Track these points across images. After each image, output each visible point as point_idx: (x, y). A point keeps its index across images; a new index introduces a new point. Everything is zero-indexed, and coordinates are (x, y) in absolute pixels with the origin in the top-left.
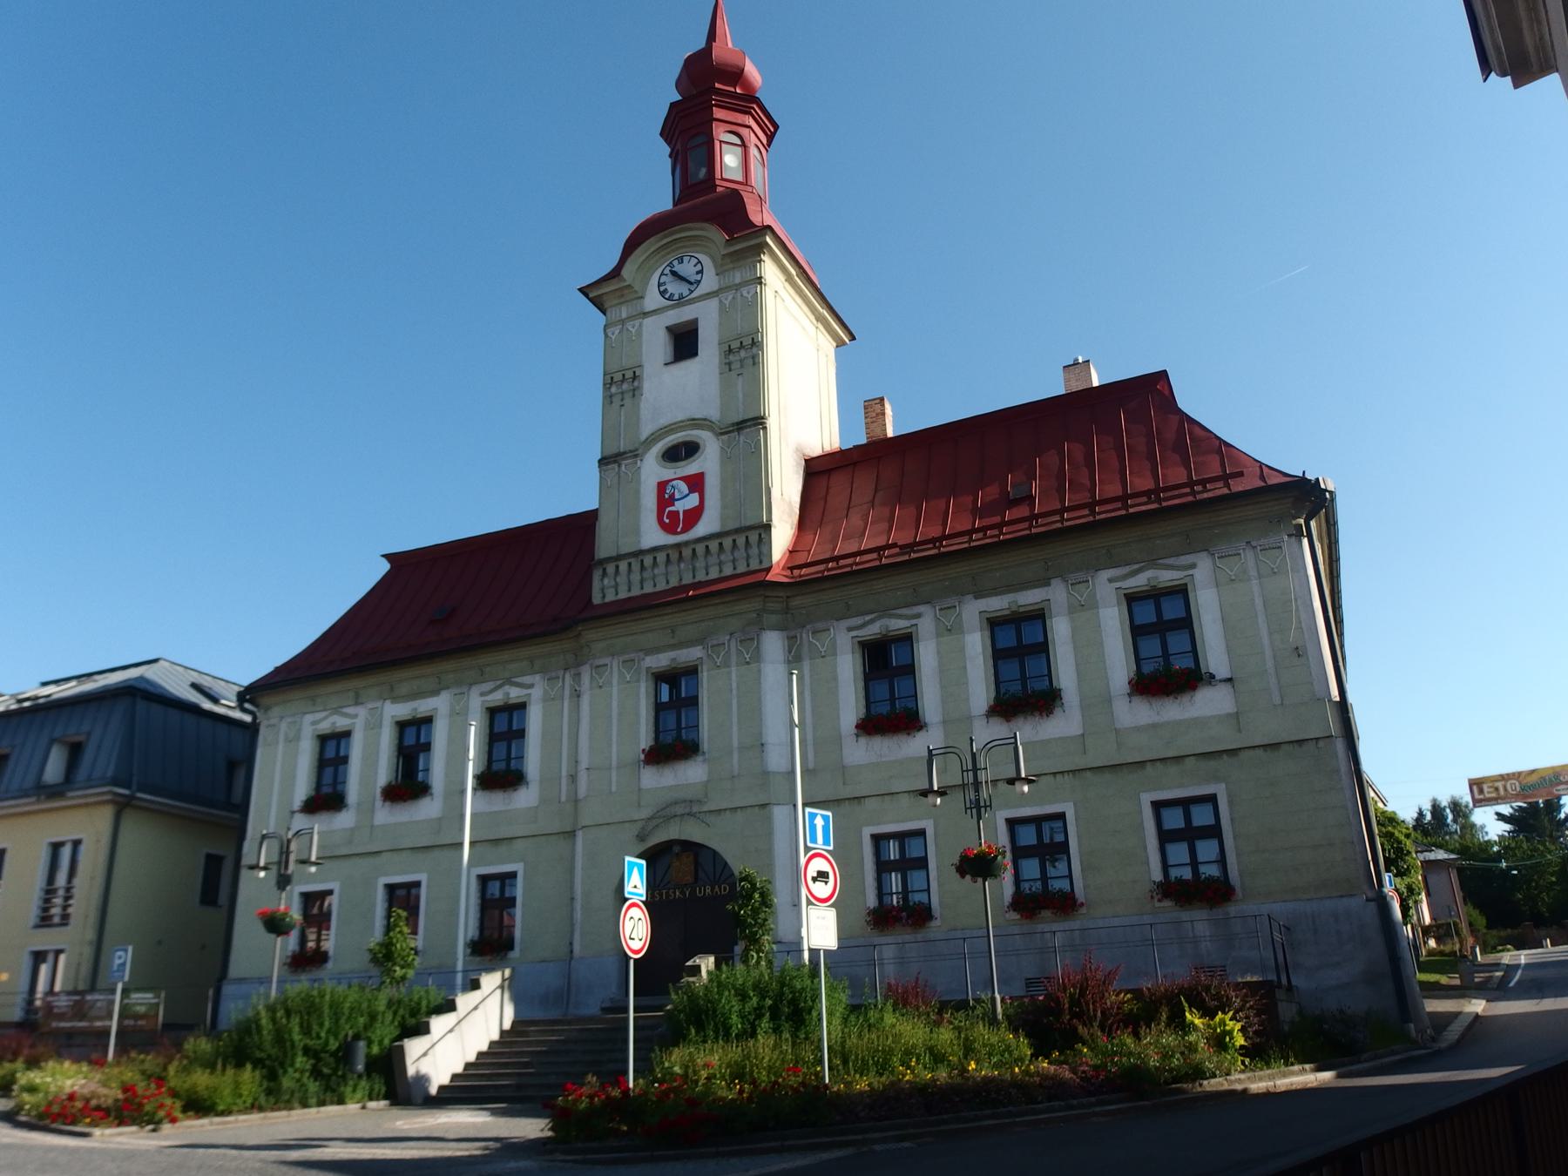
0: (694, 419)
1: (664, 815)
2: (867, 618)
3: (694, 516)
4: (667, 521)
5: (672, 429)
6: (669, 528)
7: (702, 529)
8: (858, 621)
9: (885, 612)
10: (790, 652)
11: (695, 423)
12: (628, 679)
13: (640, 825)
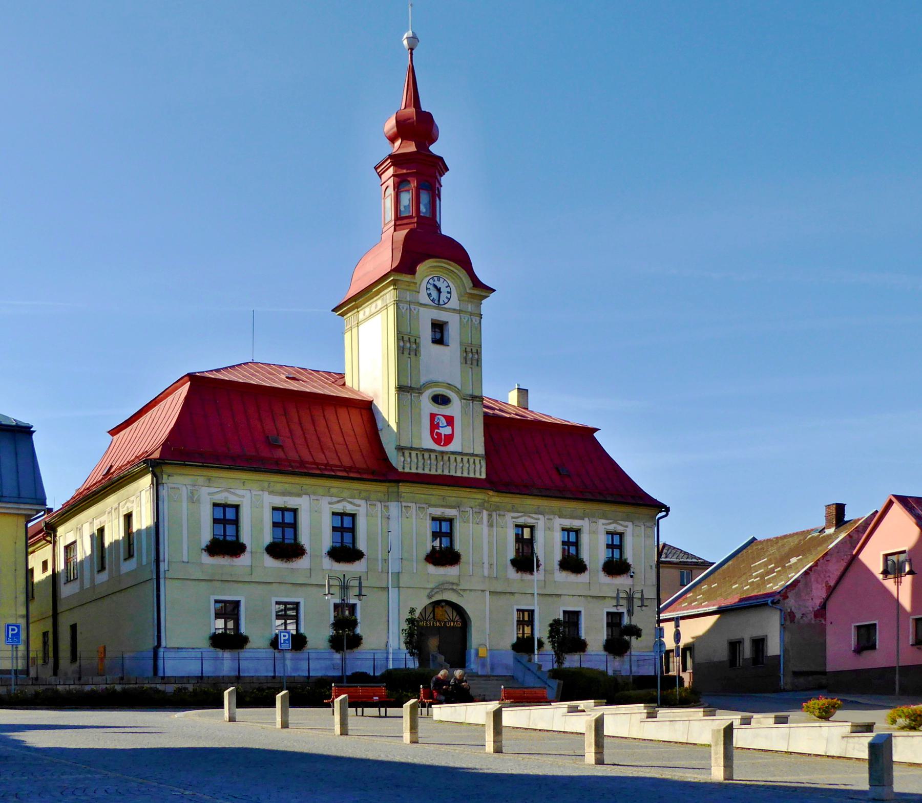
0: (449, 384)
1: (441, 587)
2: (520, 514)
3: (449, 439)
4: (436, 437)
5: (438, 385)
6: (437, 440)
7: (451, 447)
8: (516, 515)
9: (526, 513)
10: (488, 522)
11: (450, 386)
12: (422, 517)
13: (429, 591)
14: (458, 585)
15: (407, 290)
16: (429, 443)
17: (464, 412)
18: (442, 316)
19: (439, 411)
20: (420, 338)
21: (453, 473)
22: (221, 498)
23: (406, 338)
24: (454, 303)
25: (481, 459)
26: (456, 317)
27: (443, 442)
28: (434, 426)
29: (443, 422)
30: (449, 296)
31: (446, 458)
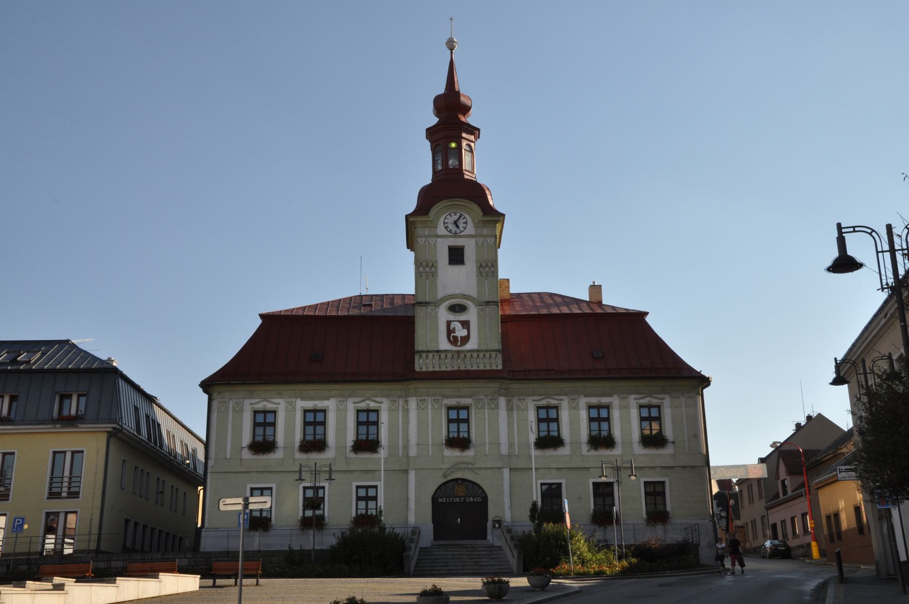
3: (465, 339)
6: (454, 341)
11: (465, 297)
12: (436, 408)
14: (472, 464)
15: (426, 227)
16: (444, 345)
17: (480, 317)
18: (458, 242)
19: (455, 318)
20: (437, 262)
21: (469, 368)
22: (260, 406)
23: (424, 264)
24: (470, 229)
25: (497, 353)
26: (473, 241)
27: (459, 343)
28: (450, 331)
29: (458, 326)
30: (465, 225)
31: (462, 355)
